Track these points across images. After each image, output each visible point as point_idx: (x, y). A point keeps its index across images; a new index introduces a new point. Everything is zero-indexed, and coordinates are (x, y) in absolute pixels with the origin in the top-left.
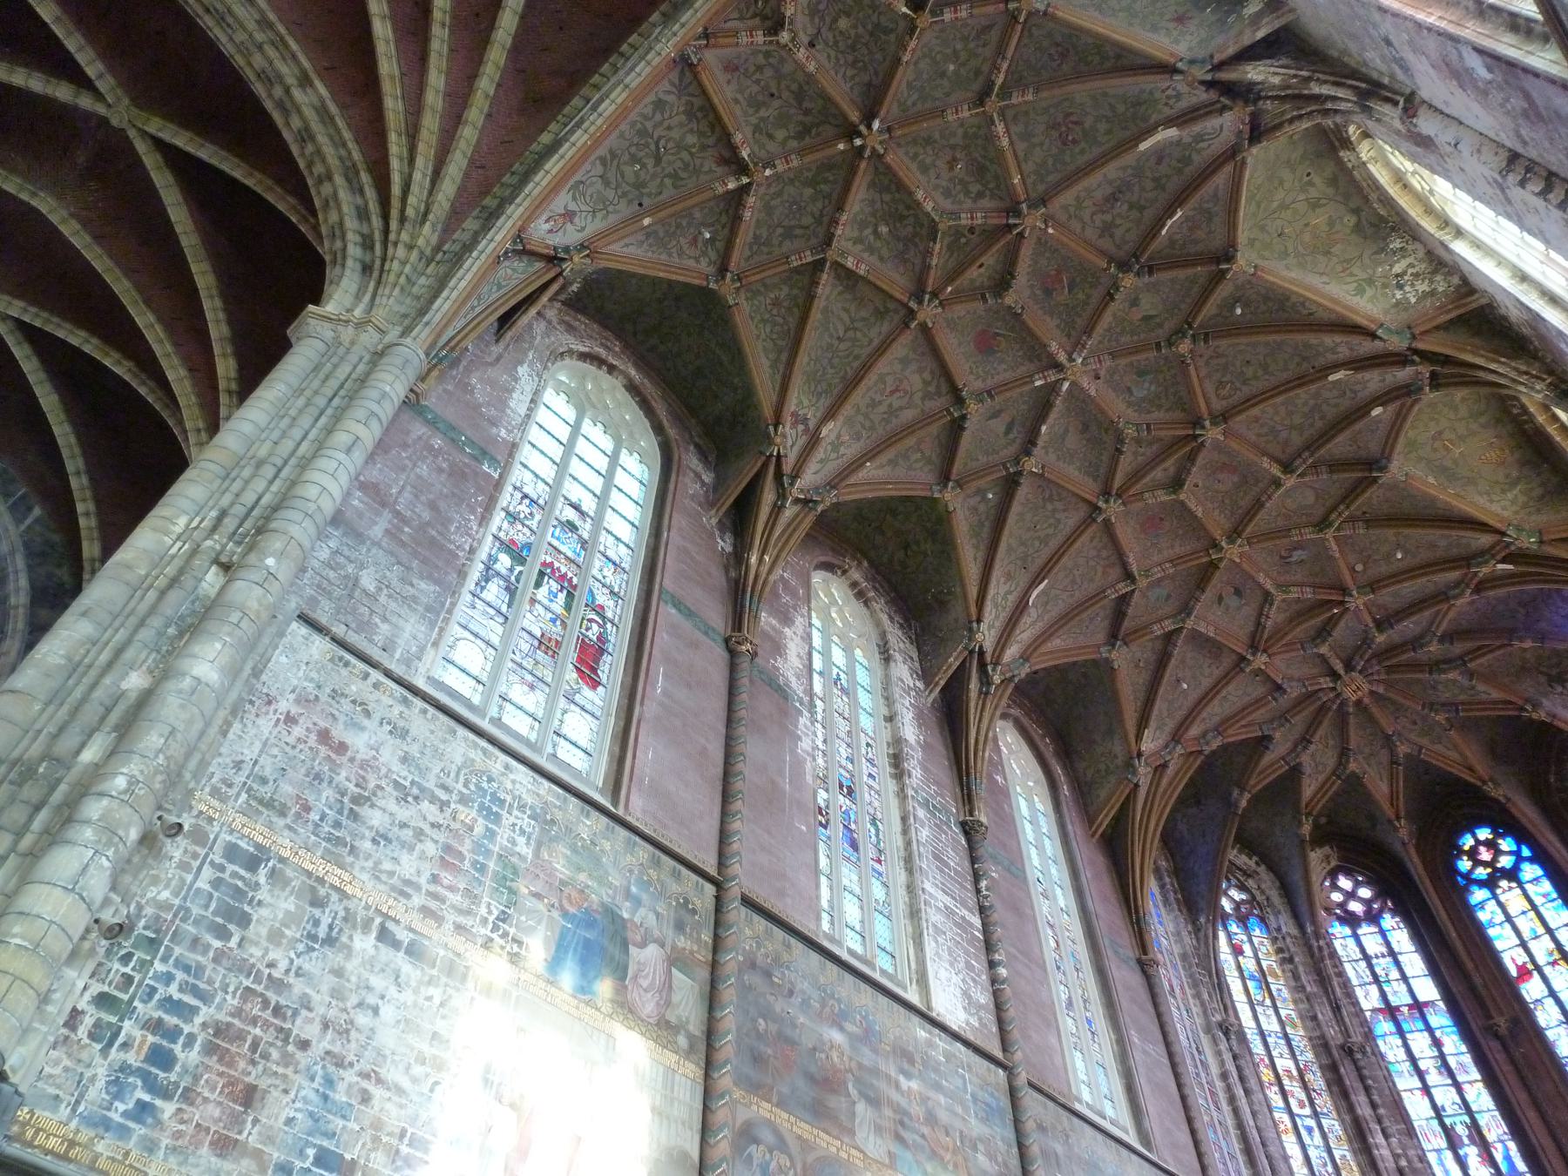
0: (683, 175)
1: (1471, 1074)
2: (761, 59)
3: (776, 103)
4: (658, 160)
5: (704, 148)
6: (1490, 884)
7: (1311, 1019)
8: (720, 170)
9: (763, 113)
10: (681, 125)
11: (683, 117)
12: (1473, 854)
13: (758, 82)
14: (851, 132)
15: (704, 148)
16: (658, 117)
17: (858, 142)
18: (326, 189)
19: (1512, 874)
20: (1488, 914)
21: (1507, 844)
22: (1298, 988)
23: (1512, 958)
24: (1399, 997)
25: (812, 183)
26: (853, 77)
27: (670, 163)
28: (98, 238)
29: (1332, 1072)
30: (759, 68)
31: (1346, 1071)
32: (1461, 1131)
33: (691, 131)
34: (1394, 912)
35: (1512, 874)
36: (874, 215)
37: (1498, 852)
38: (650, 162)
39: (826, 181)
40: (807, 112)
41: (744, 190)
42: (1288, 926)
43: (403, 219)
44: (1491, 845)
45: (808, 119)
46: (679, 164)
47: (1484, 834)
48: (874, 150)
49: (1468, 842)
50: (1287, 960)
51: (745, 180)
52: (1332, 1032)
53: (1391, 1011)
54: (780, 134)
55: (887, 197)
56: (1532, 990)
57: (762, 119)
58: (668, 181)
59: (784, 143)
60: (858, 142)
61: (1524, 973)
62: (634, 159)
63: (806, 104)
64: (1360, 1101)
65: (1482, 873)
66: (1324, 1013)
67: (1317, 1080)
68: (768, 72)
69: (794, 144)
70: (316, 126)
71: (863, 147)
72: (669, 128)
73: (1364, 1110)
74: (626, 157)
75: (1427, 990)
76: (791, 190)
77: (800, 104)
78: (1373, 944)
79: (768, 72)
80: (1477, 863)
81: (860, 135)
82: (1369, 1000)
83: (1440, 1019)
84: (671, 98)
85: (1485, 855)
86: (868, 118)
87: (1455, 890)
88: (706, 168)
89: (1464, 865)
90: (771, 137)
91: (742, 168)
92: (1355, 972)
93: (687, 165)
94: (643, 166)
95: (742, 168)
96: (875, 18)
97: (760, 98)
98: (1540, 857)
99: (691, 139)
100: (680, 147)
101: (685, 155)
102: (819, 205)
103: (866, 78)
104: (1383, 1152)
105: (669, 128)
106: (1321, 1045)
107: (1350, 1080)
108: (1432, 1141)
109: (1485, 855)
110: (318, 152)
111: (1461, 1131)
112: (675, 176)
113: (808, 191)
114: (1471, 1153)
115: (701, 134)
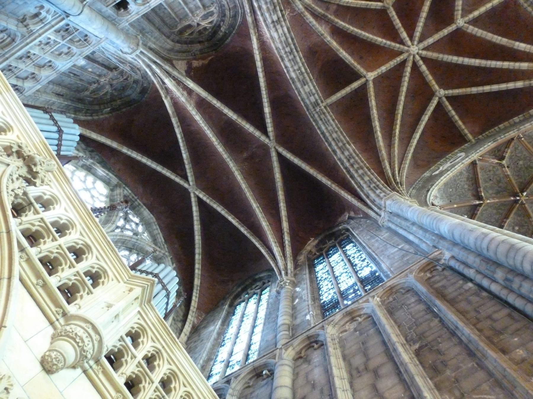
0: (462, 196)
2: (491, 168)
3: (491, 182)
4: (456, 190)
5: (469, 190)
8: (472, 198)
9: (487, 184)
10: (464, 181)
11: (466, 179)
13: (488, 175)
14: (515, 195)
15: (469, 190)
16: (459, 177)
17: (518, 198)
25: (497, 209)
26: (517, 180)
27: (459, 192)
28: (245, 178)
30: (490, 171)
33: (467, 184)
36: (514, 223)
38: (454, 189)
39: (501, 209)
40: (500, 187)
41: (480, 205)
45: (499, 189)
46: (461, 193)
48: (522, 202)
51: (482, 202)
54: (490, 192)
55: (519, 218)
57: (486, 186)
58: (458, 197)
59: (491, 195)
60: (518, 198)
62: (451, 188)
63: (501, 184)
68: (492, 173)
69: (494, 195)
71: (518, 200)
72: (461, 181)
74: (449, 186)
76: (490, 209)
77: (498, 184)
79: (492, 173)
81: (519, 196)
84: (464, 172)
86: (522, 191)
88: (468, 196)
90: (487, 192)
91: (480, 198)
93: (463, 193)
94: (452, 190)
95: (480, 198)
96: (529, 163)
97: (487, 180)
99: (466, 186)
100: (463, 188)
101: (464, 192)
102: (498, 216)
103: (521, 180)
105: (461, 181)
112: (459, 196)
113: (495, 211)
115: (469, 186)
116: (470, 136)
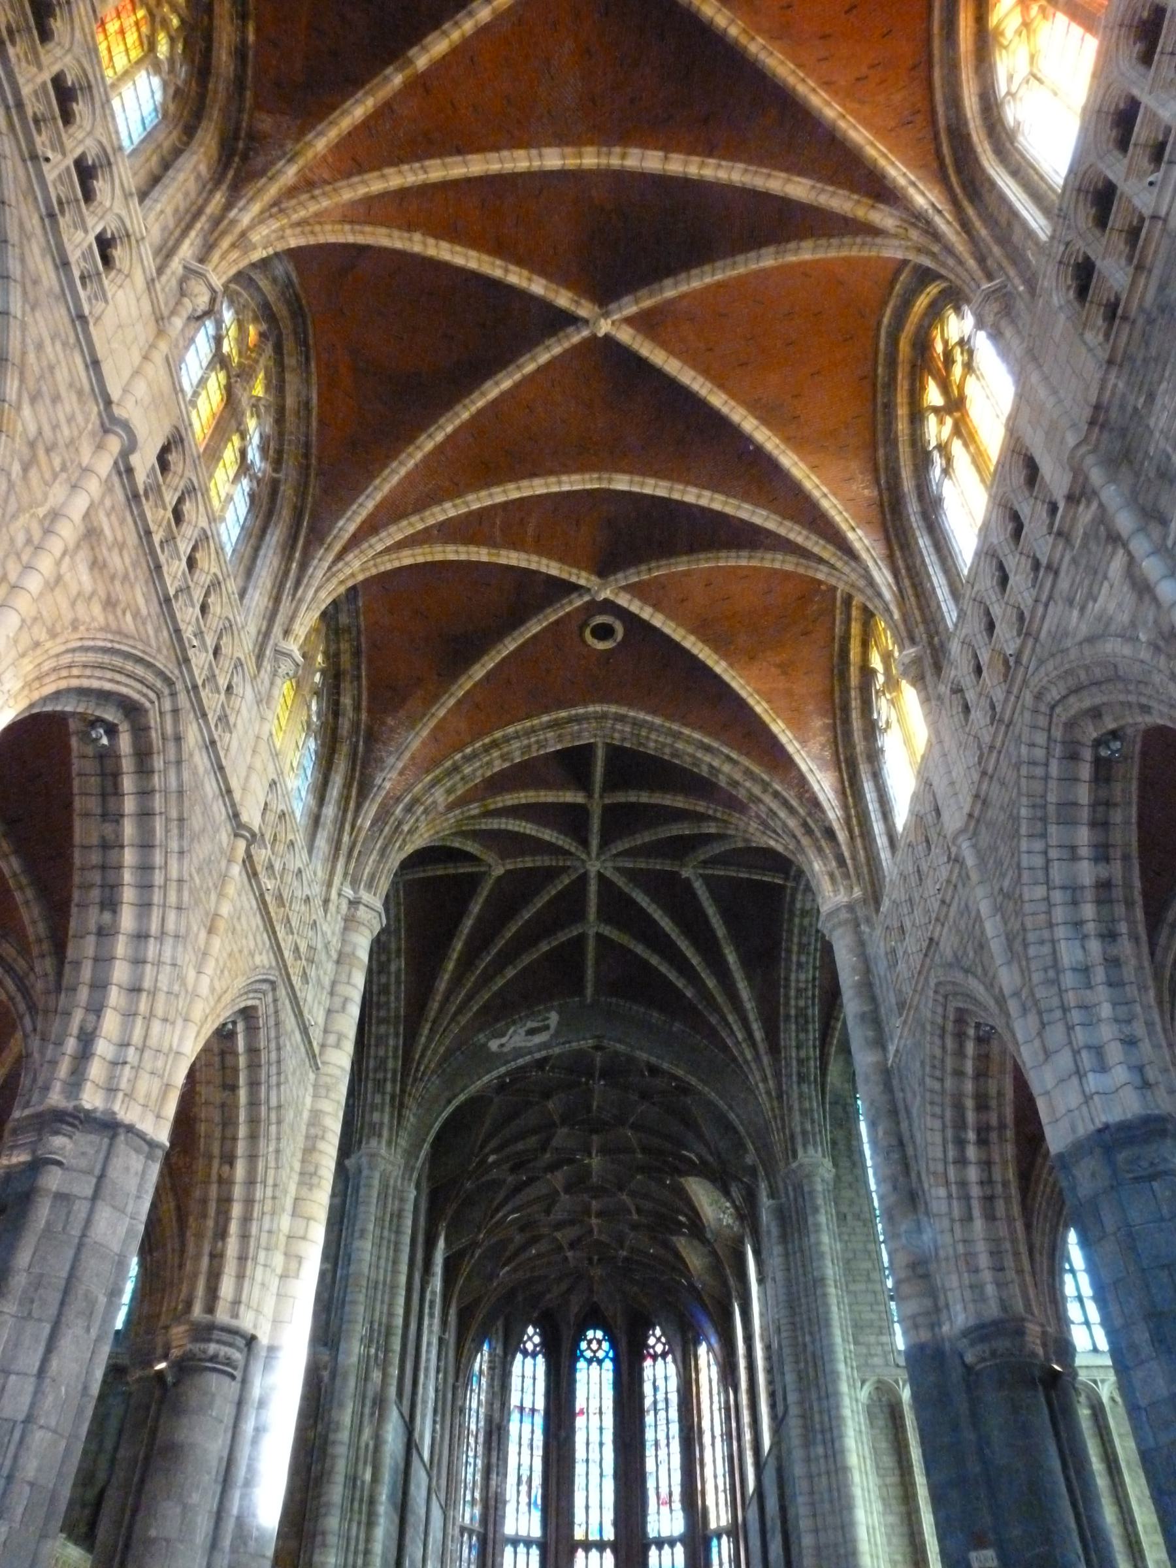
1: (539, 1452)
6: (590, 1361)
7: (490, 1404)
12: (590, 1342)
18: (383, 1029)
19: (600, 1362)
20: (581, 1376)
21: (606, 1345)
22: (491, 1385)
23: (580, 1403)
24: (527, 1405)
29: (489, 1435)
31: (495, 1438)
32: (524, 1479)
34: (545, 1356)
35: (600, 1362)
37: (600, 1348)
42: (499, 1351)
43: (415, 1080)
44: (599, 1342)
47: (599, 1334)
49: (590, 1334)
50: (491, 1368)
52: (497, 1415)
53: (521, 1409)
56: (580, 1422)
61: (582, 1412)
64: (494, 1454)
65: (588, 1354)
66: (497, 1405)
67: (481, 1439)
70: (393, 988)
73: (494, 1460)
75: (540, 1404)
78: (529, 1372)
80: (589, 1348)
82: (515, 1400)
83: (539, 1420)
85: (594, 1346)
87: (574, 1357)
89: (583, 1345)
92: (515, 1382)
98: (615, 1360)
104: (493, 1483)
106: (489, 1419)
107: (494, 1444)
108: (512, 1479)
109: (594, 1346)
110: (388, 1003)
111: (524, 1479)
114: (524, 1488)
116: (589, 991)
